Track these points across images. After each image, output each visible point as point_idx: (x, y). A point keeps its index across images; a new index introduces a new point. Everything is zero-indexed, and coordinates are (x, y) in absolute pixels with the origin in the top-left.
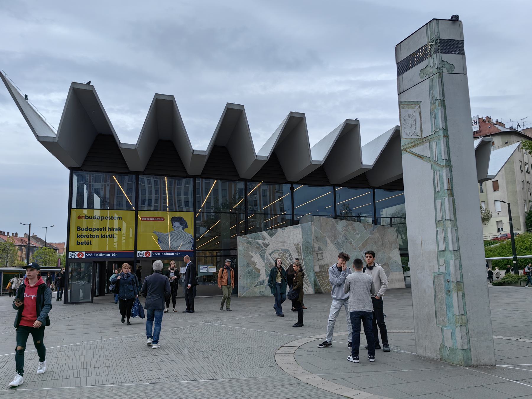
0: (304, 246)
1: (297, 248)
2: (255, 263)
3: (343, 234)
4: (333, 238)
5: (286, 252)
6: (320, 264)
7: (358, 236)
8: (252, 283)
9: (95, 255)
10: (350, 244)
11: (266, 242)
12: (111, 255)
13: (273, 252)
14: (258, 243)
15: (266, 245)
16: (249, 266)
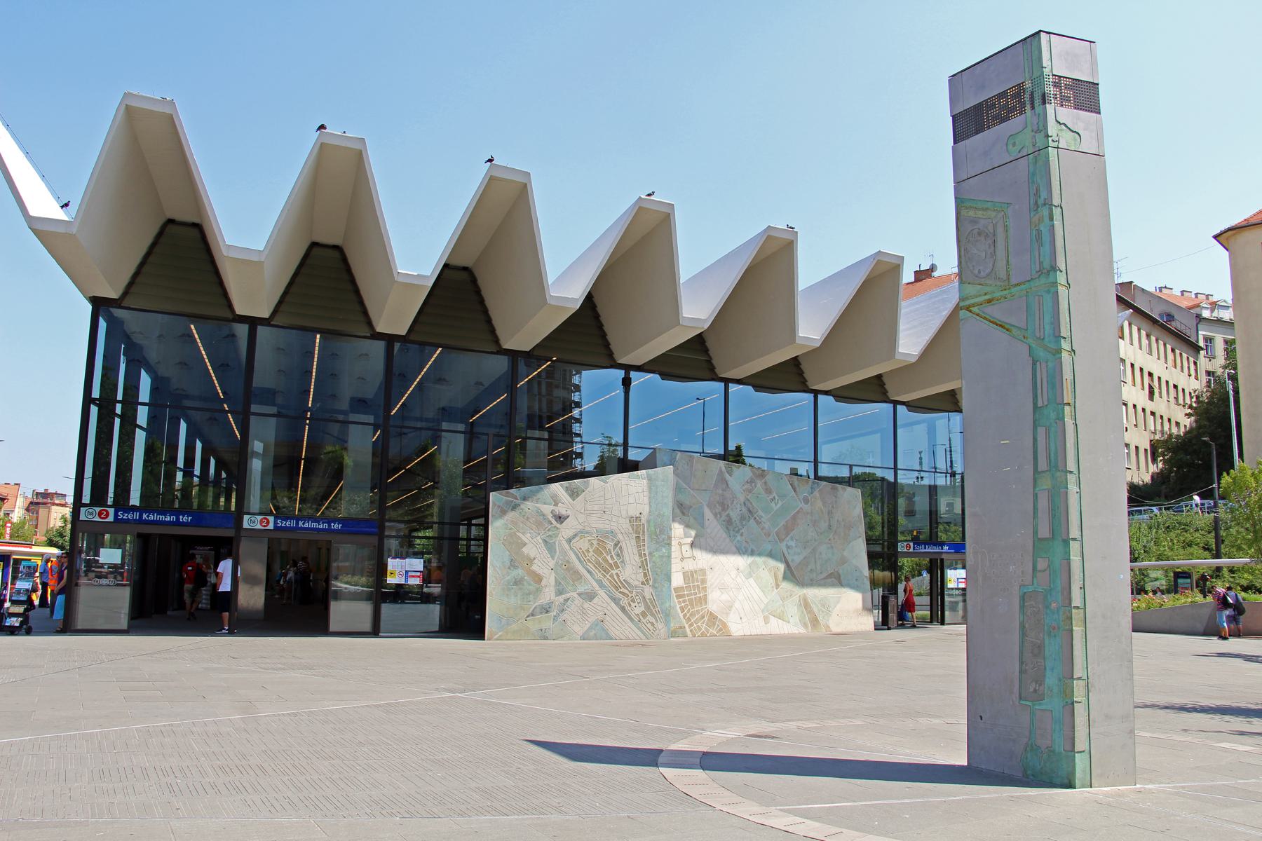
0: (652, 524)
3: (742, 500)
4: (719, 509)
5: (607, 537)
6: (686, 569)
8: (522, 608)
9: (141, 516)
10: (758, 523)
11: (561, 510)
12: (178, 519)
13: (575, 536)
15: (560, 518)
16: (515, 567)
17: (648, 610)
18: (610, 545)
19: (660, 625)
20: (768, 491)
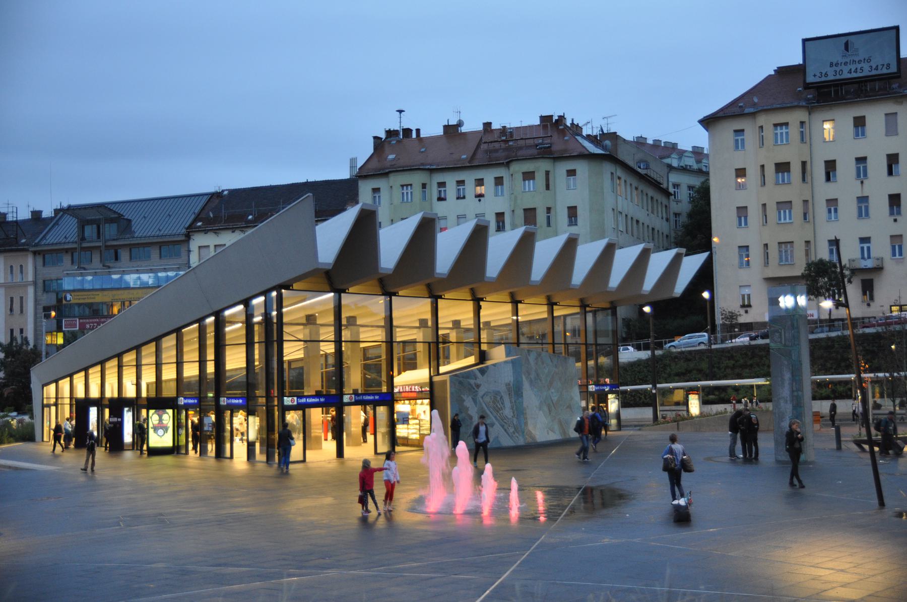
1: (509, 390)
2: (467, 409)
7: (546, 371)
11: (478, 382)
14: (470, 384)
15: (478, 386)
17: (516, 430)
18: (499, 398)
19: (520, 437)
20: (543, 363)
